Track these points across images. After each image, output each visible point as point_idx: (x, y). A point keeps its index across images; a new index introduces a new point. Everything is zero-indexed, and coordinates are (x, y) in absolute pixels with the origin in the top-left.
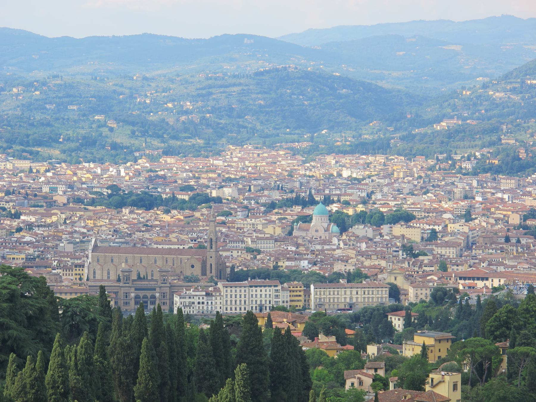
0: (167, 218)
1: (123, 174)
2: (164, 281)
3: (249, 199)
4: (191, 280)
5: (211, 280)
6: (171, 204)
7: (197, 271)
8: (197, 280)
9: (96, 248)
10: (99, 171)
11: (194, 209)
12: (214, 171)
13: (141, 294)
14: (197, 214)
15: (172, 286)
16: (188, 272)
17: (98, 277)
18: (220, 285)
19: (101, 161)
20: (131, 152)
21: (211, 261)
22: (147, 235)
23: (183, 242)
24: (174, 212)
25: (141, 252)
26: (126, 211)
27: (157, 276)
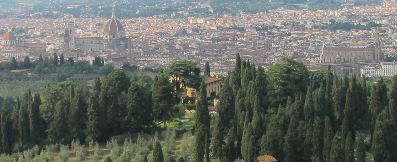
0: (356, 34)
1: (336, 15)
2: (356, 63)
3: (394, 24)
4: (368, 62)
5: (377, 62)
6: (358, 28)
7: (371, 57)
8: (370, 62)
9: (325, 48)
10: (326, 14)
11: (369, 30)
12: (377, 12)
13: (346, 68)
14: (371, 32)
15: (359, 65)
16: (367, 58)
17: (326, 61)
18: (381, 64)
19: (326, 9)
20: (340, 5)
21: (377, 53)
22: (348, 42)
23: (364, 45)
24: (360, 31)
25: (345, 49)
26: (338, 31)
27: (353, 60)
